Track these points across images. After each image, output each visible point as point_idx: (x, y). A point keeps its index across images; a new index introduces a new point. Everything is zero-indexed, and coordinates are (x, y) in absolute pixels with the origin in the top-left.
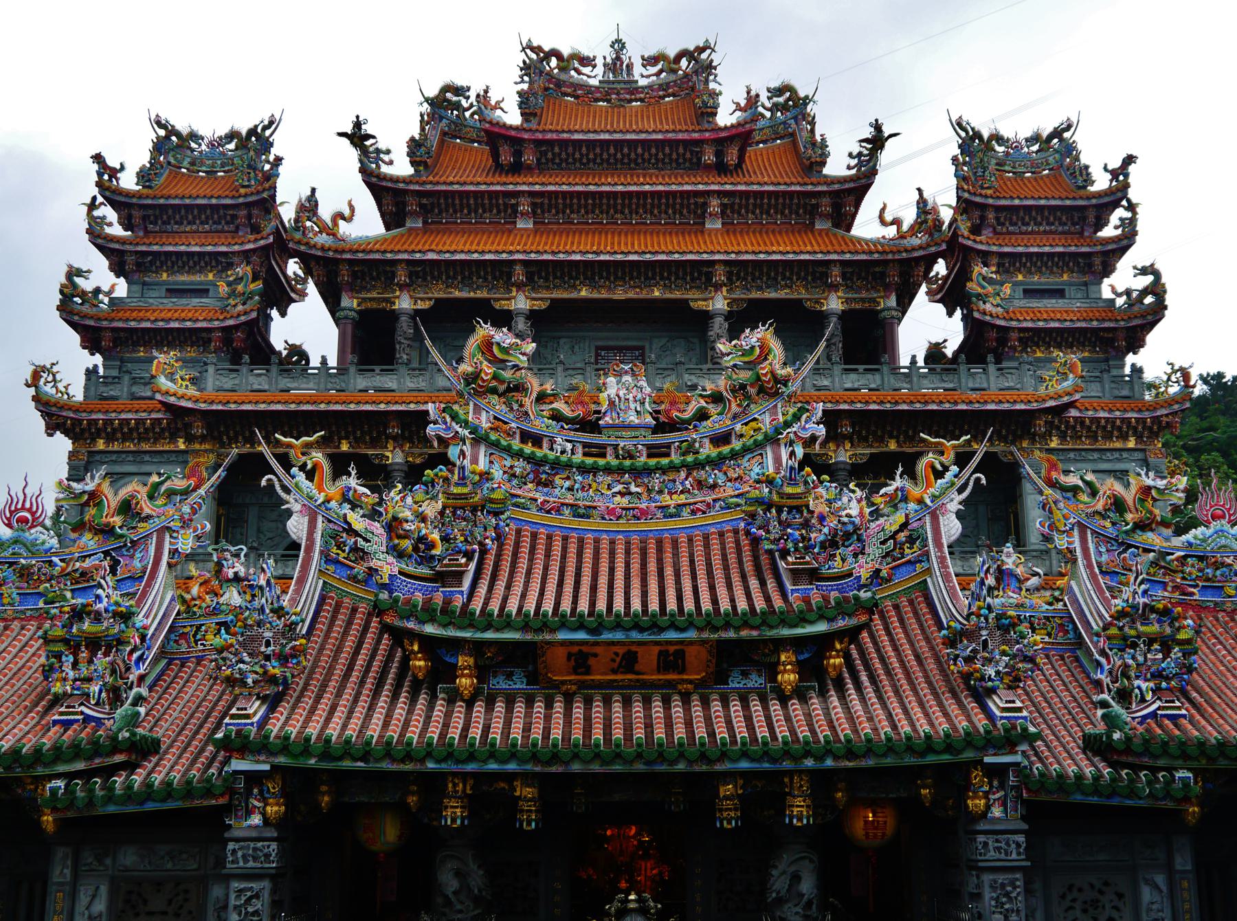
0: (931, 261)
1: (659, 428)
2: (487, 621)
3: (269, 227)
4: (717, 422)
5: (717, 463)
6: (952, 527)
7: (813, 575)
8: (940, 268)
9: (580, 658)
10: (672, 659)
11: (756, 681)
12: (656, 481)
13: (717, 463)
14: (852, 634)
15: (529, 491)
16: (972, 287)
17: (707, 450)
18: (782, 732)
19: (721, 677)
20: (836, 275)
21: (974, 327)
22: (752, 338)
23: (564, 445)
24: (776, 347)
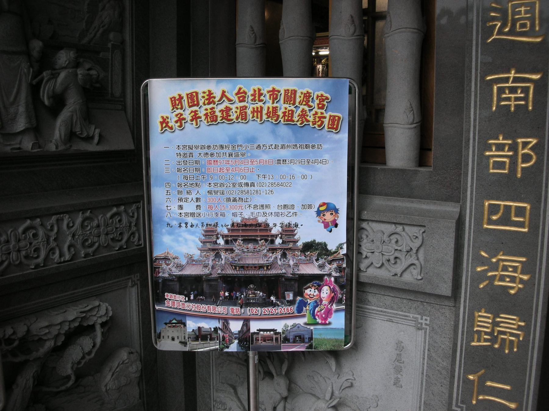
0: (279, 235)
1: (254, 249)
2: (240, 264)
3: (217, 232)
4: (259, 248)
5: (259, 251)
6: (280, 257)
7: (268, 260)
8: (280, 235)
9: (247, 267)
10: (255, 267)
11: (263, 269)
12: (254, 253)
13: (259, 251)
14: (271, 265)
15: (243, 254)
16: (283, 237)
17: (258, 251)
18: (265, 273)
19: (260, 269)
20: (270, 236)
21: (283, 241)
22: (262, 241)
23: (245, 250)
24: (264, 242)
